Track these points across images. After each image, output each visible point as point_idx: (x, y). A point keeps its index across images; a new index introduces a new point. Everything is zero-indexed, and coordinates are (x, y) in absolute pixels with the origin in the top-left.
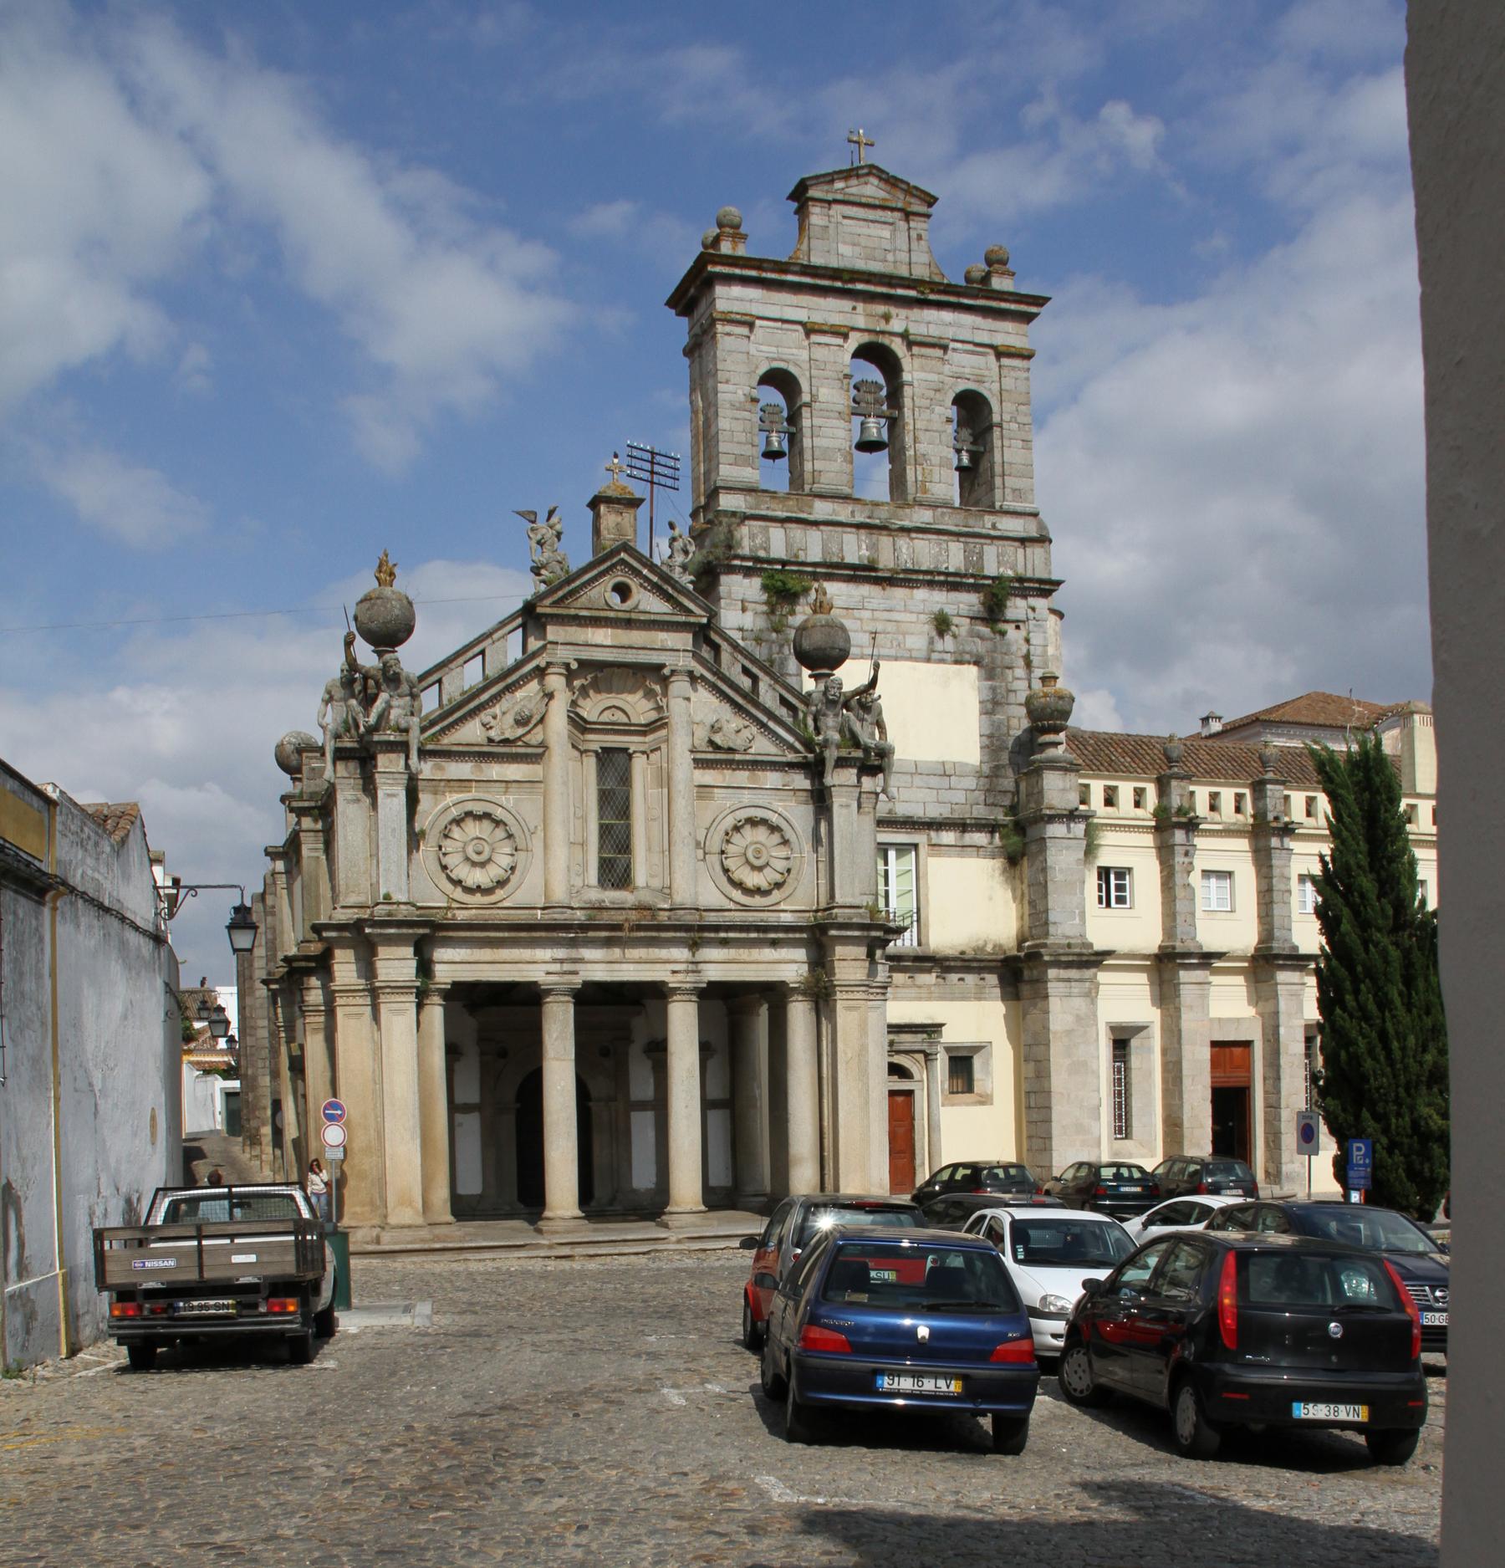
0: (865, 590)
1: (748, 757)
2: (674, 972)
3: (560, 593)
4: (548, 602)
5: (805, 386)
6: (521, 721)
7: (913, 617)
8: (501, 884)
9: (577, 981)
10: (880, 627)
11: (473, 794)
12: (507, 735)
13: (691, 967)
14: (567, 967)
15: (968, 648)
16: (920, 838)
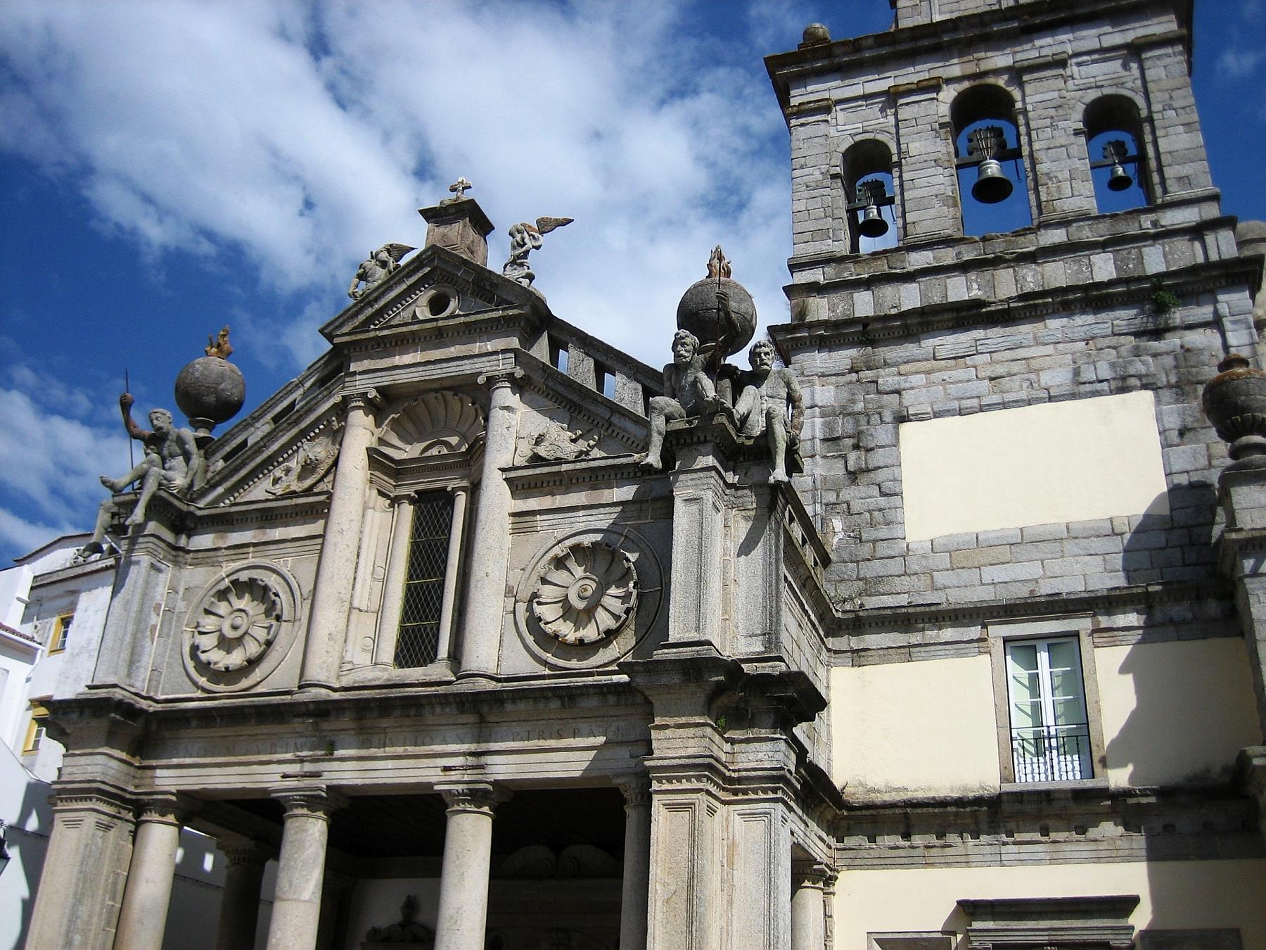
0: (978, 334)
2: (446, 769)
3: (361, 317)
4: (346, 329)
5: (894, 149)
6: (308, 467)
7: (1049, 349)
8: (252, 663)
9: (322, 783)
10: (1000, 370)
11: (251, 561)
12: (293, 488)
13: (471, 761)
14: (308, 767)
15: (1132, 371)
16: (1082, 624)
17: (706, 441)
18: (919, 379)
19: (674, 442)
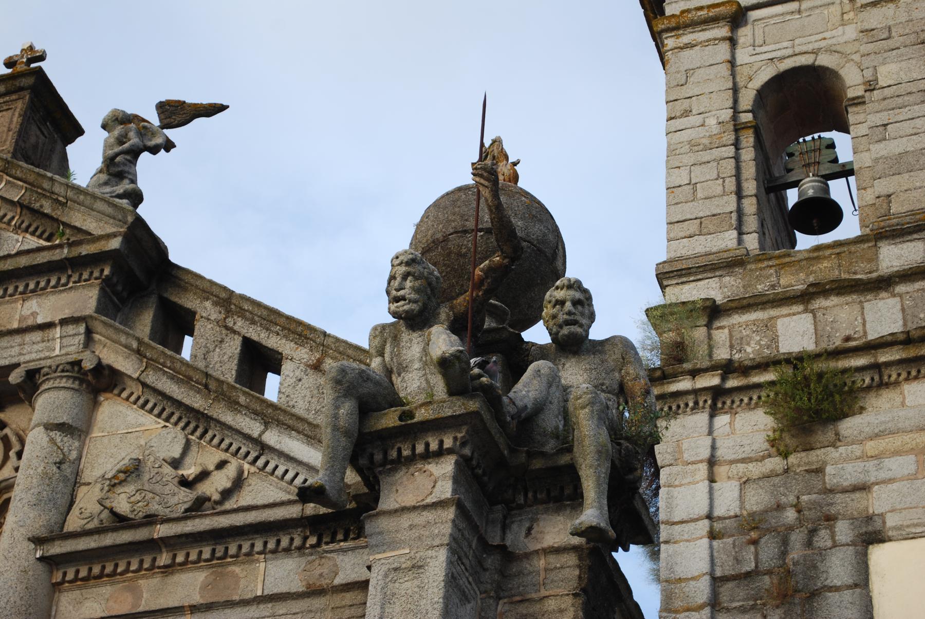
1: (190, 526)
17: (441, 453)
18: (903, 465)
19: (378, 457)
